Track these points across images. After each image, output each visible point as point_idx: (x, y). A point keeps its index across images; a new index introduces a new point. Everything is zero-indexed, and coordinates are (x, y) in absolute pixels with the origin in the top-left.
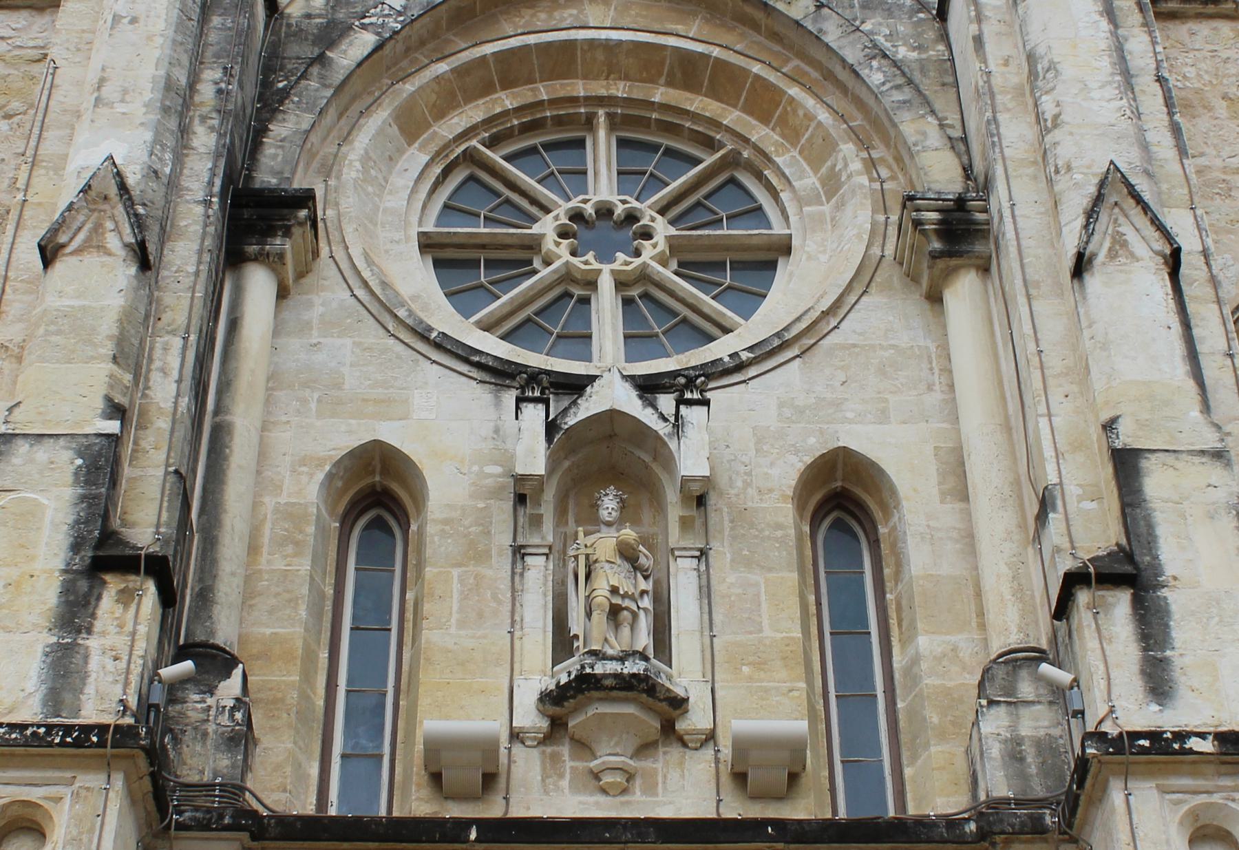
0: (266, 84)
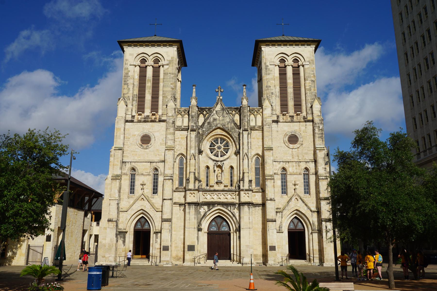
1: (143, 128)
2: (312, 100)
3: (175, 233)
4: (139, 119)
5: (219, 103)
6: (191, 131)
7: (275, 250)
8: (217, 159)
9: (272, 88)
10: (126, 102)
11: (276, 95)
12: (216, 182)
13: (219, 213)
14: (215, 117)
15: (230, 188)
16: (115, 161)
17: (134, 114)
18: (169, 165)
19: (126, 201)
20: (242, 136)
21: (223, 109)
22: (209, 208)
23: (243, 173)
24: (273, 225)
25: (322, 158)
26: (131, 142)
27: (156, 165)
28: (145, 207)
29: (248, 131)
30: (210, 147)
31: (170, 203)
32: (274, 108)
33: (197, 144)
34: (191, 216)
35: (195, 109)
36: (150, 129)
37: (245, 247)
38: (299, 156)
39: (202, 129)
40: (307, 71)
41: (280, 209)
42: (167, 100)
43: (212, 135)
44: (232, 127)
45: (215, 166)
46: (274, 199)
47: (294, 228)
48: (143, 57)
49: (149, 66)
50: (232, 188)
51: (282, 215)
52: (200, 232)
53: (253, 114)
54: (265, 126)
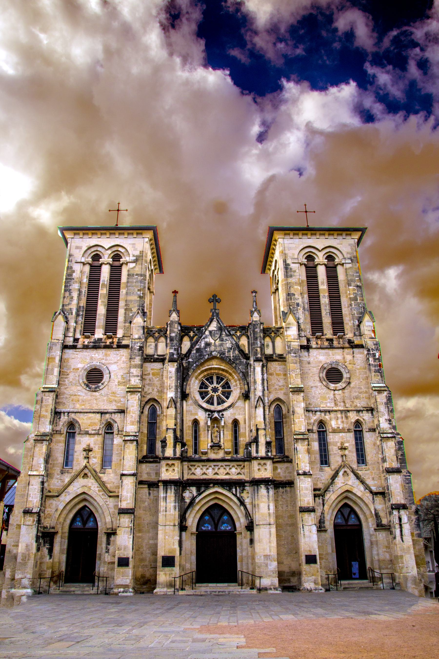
0: (183, 376)
1: (92, 358)
2: (360, 315)
3: (140, 534)
4: (86, 343)
5: (215, 320)
6: (169, 361)
7: (315, 562)
8: (212, 408)
9: (296, 296)
10: (66, 318)
11: (304, 308)
12: (211, 446)
13: (216, 498)
14: (208, 340)
15: (235, 456)
16: (43, 409)
17: (78, 336)
18: (132, 416)
19: (57, 479)
20: (252, 370)
21: (220, 329)
22: (198, 490)
23: (257, 430)
24: (310, 518)
25: (384, 404)
26: (71, 380)
27: (110, 418)
28: (90, 488)
29: (262, 361)
30: (200, 389)
31: (132, 481)
32: (302, 326)
33: (178, 383)
34: (168, 504)
35: (176, 327)
36: (103, 359)
37: (263, 557)
38: (346, 401)
39: (187, 360)
40: (350, 272)
41: (319, 490)
42: (131, 315)
43: (204, 368)
44: (236, 356)
45: (209, 419)
46: (309, 472)
47: (344, 523)
48: (97, 251)
49: (106, 264)
50: (238, 456)
51: (323, 500)
52: (184, 533)
53: (268, 336)
54: (290, 355)
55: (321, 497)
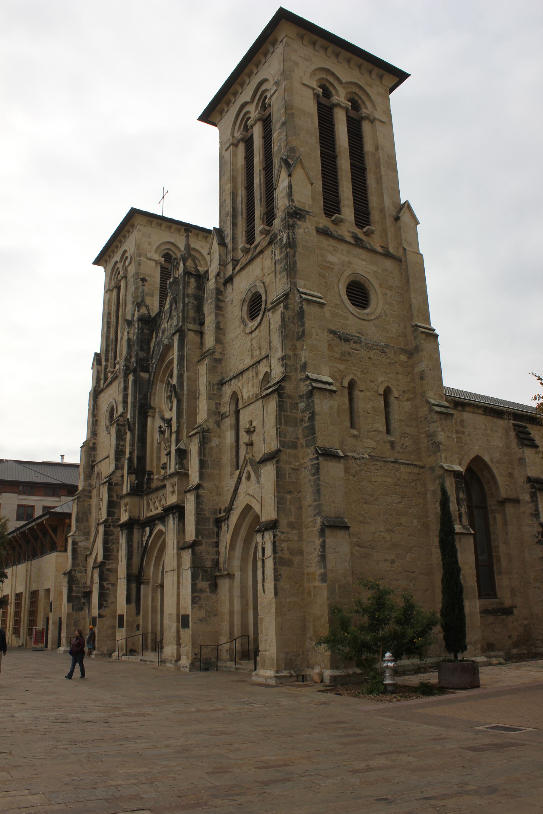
51: (228, 528)
55: (226, 521)
